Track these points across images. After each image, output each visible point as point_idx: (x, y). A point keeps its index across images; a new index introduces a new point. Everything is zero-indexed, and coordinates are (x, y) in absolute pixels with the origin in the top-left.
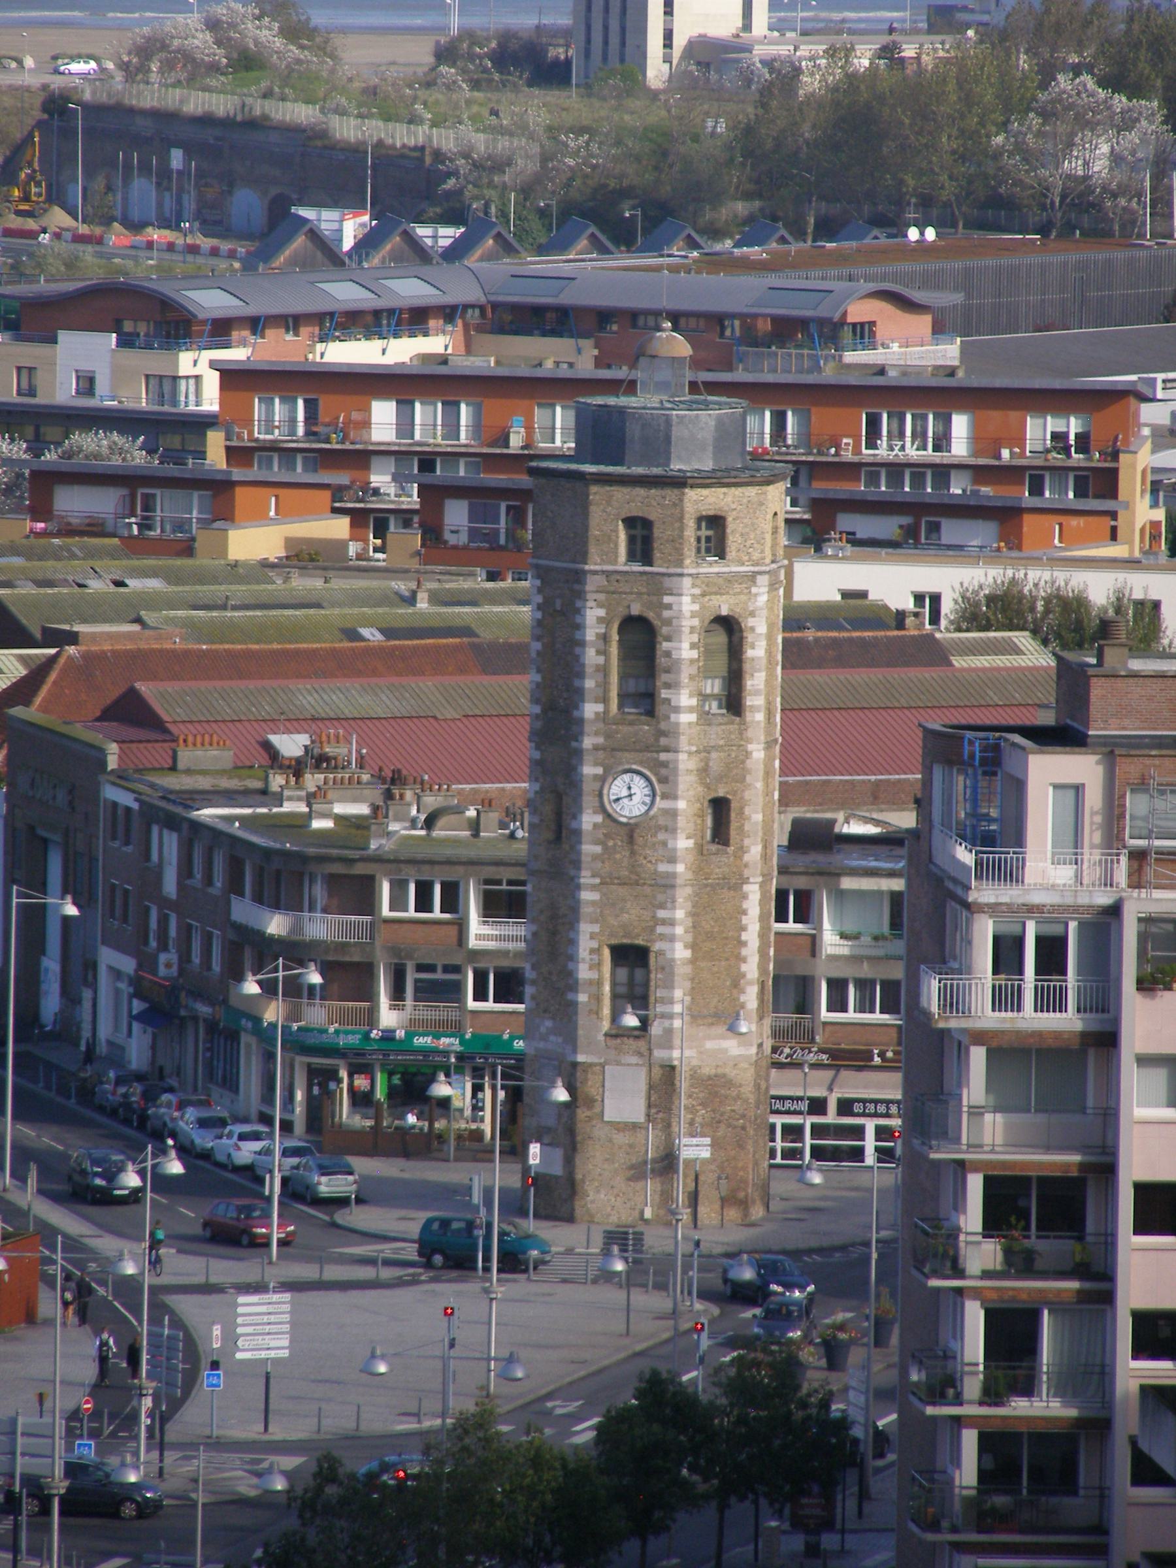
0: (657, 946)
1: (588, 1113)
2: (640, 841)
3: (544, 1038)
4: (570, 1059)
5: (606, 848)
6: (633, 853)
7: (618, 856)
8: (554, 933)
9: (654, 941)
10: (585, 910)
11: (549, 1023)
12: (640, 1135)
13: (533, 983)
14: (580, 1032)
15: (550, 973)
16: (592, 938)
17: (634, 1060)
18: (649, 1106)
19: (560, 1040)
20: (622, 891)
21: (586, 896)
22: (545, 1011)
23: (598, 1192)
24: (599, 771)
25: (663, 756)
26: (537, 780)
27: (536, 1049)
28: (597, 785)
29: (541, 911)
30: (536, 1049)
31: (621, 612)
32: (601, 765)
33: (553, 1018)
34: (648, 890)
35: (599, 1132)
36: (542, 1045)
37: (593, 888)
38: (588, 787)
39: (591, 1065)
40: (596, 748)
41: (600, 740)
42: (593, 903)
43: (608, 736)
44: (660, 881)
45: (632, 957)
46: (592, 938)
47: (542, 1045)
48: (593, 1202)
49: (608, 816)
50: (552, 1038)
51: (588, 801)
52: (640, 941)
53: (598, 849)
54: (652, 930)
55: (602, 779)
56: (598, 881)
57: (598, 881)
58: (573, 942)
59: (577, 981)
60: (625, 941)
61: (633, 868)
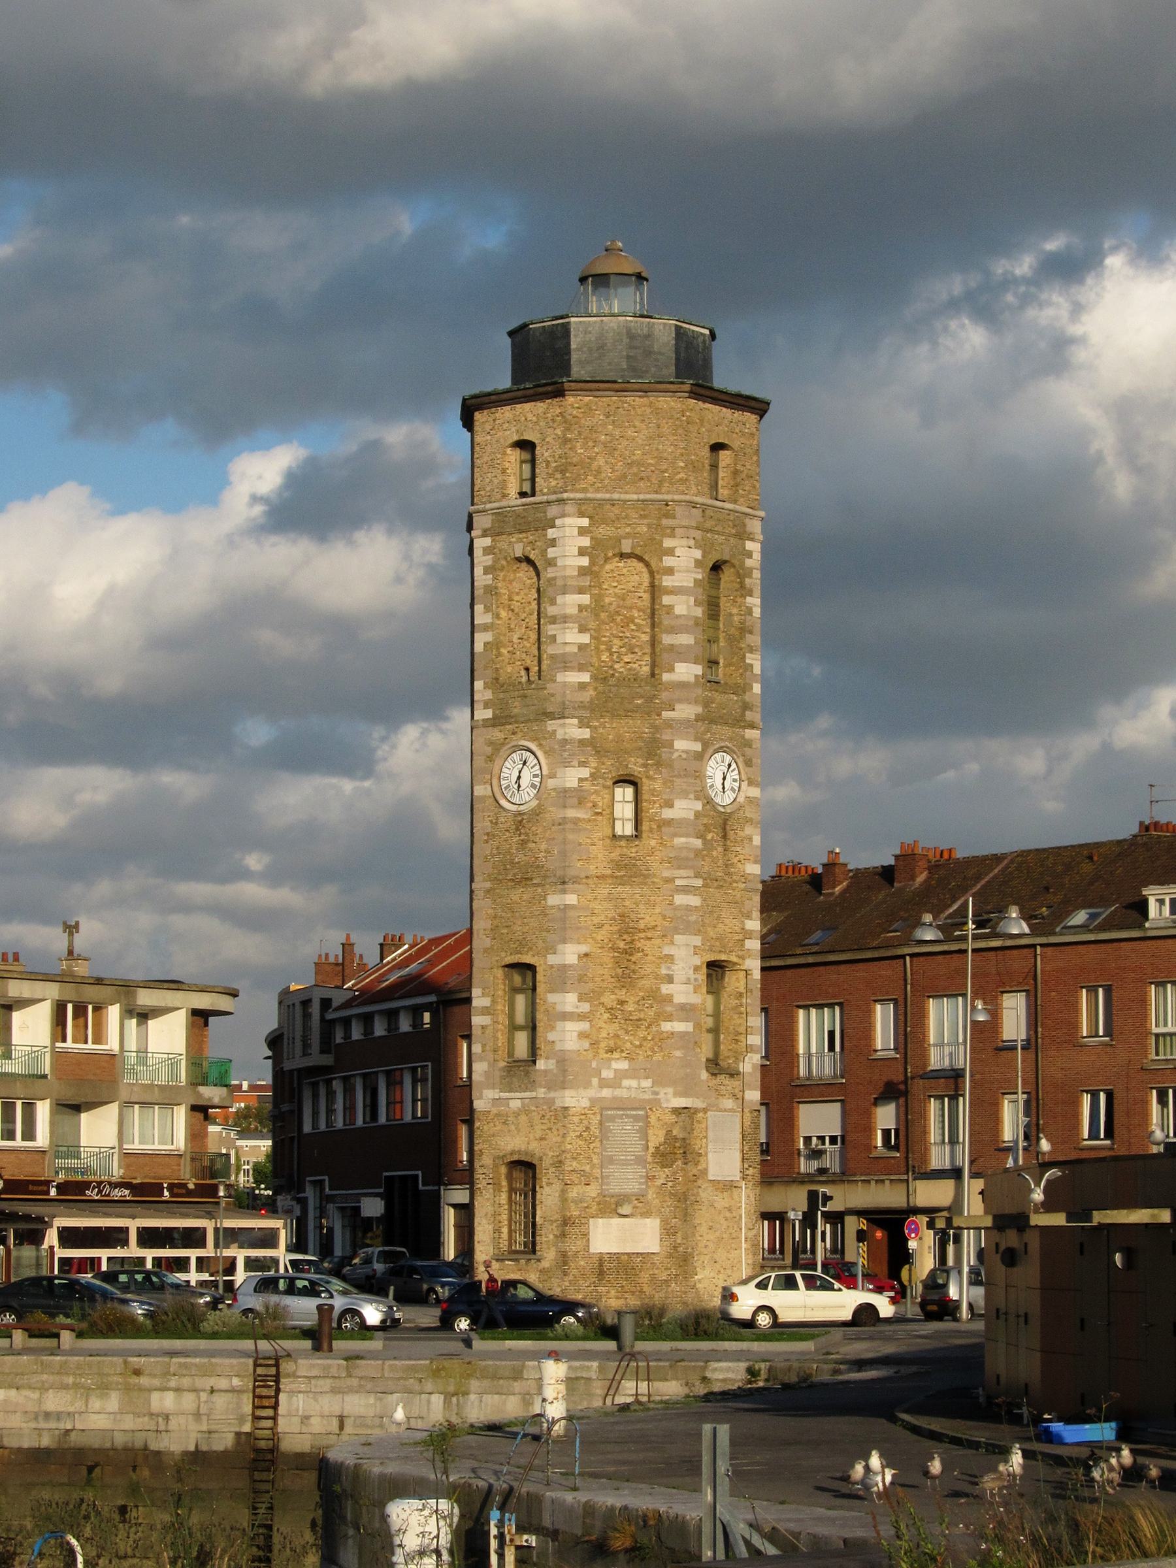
1: (695, 1171)
3: (604, 1084)
7: (714, 853)
8: (628, 952)
9: (743, 958)
11: (623, 1065)
12: (735, 1192)
13: (581, 1017)
19: (647, 1083)
22: (611, 1051)
24: (698, 747)
26: (582, 764)
33: (629, 1058)
36: (606, 1093)
47: (606, 1093)
48: (700, 1281)
50: (634, 1083)
52: (734, 959)
55: (700, 757)
56: (699, 882)
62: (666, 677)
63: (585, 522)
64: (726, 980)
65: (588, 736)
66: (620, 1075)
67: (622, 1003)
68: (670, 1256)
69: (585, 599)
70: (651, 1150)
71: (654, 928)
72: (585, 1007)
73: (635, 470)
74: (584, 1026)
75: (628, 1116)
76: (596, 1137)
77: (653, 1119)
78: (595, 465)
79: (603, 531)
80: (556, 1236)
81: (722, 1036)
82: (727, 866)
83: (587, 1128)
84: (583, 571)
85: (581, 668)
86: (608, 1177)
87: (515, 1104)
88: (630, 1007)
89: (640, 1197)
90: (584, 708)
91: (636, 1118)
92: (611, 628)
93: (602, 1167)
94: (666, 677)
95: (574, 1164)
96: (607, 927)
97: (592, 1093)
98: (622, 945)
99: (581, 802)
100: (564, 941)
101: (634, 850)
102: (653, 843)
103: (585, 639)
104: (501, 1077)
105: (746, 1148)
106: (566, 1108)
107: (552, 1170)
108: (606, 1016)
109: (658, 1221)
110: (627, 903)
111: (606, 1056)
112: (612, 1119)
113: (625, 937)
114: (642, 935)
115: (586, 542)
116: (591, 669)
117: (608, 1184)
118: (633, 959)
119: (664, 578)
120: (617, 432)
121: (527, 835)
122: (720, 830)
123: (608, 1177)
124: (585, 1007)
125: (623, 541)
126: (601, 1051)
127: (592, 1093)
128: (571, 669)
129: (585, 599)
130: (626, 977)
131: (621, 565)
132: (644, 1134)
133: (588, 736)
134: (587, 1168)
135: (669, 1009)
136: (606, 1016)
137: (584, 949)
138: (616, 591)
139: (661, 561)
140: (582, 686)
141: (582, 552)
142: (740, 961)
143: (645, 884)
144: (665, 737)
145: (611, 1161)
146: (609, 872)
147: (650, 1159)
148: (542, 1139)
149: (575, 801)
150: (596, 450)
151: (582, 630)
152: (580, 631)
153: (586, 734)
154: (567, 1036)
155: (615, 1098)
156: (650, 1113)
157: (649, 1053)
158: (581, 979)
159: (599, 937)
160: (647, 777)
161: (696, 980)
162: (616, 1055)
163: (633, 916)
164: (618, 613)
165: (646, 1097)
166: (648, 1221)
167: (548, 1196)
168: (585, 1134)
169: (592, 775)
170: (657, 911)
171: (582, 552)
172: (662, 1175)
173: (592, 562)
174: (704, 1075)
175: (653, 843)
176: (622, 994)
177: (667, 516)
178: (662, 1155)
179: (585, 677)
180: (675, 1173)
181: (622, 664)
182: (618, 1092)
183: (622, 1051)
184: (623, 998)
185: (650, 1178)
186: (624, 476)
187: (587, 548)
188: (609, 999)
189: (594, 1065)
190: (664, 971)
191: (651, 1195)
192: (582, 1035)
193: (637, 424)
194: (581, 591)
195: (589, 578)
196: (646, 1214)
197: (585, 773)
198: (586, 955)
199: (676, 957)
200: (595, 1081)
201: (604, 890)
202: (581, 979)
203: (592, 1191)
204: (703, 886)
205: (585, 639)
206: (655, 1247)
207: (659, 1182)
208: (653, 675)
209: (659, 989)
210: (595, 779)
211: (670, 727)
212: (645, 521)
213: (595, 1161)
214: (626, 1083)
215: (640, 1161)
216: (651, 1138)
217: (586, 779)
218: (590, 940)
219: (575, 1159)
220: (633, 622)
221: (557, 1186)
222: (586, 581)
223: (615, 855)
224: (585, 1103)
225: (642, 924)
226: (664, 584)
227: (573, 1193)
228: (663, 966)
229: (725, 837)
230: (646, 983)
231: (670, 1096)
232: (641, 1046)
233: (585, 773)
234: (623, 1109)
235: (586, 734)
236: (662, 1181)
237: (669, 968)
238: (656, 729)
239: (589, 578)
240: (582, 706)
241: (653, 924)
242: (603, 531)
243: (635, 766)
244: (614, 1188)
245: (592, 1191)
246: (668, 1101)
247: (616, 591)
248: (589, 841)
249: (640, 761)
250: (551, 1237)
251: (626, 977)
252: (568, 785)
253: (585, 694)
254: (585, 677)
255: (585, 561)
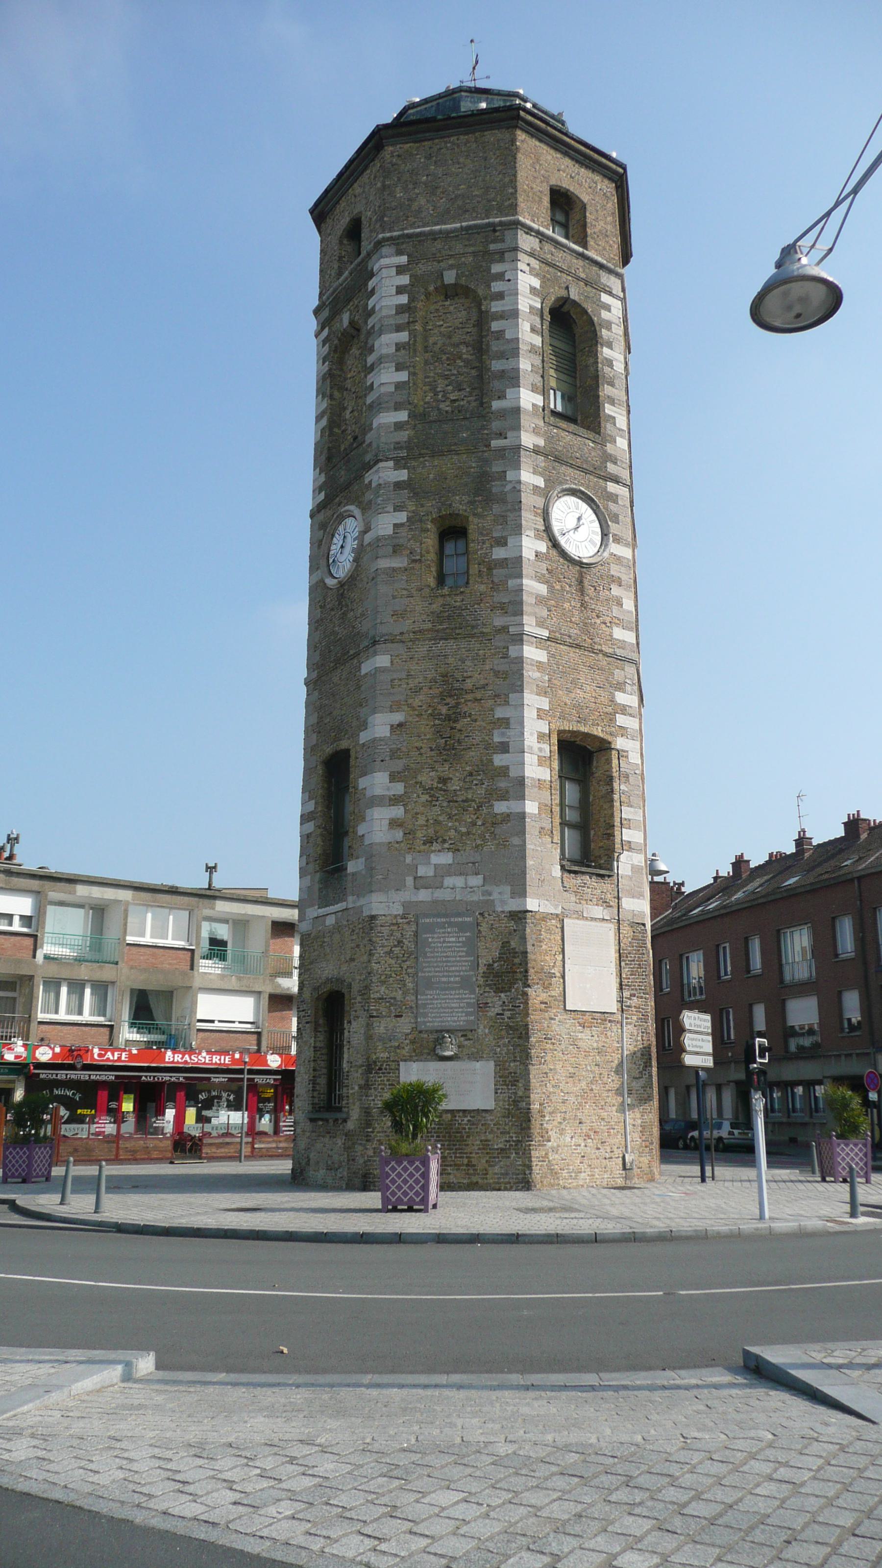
0: (620, 743)
1: (543, 996)
2: (591, 591)
3: (420, 883)
4: (513, 905)
5: (551, 588)
6: (584, 605)
8: (453, 718)
10: (531, 674)
11: (445, 858)
13: (394, 801)
14: (530, 862)
15: (444, 780)
16: (539, 717)
17: (598, 911)
18: (621, 987)
19: (476, 881)
20: (573, 655)
21: (532, 653)
22: (429, 841)
23: (562, 1132)
25: (612, 487)
26: (398, 509)
27: (405, 905)
28: (540, 502)
29: (417, 690)
30: (405, 905)
31: (557, 292)
32: (541, 474)
34: (604, 661)
35: (560, 1026)
36: (424, 895)
37: (540, 642)
38: (528, 500)
39: (545, 917)
40: (537, 451)
41: (541, 442)
42: (539, 665)
43: (549, 439)
44: (619, 652)
45: (583, 758)
46: (539, 717)
47: (424, 895)
48: (555, 1150)
49: (555, 544)
50: (459, 881)
51: (529, 520)
52: (598, 732)
53: (543, 589)
54: (612, 720)
57: (546, 633)
58: (512, 723)
59: (521, 782)
60: (583, 729)
61: (586, 627)
62: (496, 405)
63: (404, 259)
64: (595, 763)
65: (405, 478)
66: (442, 872)
67: (444, 780)
68: (508, 1114)
69: (404, 336)
70: (482, 969)
71: (483, 687)
72: (399, 788)
73: (460, 203)
74: (398, 812)
75: (451, 924)
76: (411, 953)
77: (484, 928)
78: (415, 206)
79: (422, 268)
80: (361, 1087)
81: (592, 832)
82: (585, 624)
83: (399, 942)
84: (401, 309)
85: (397, 407)
86: (425, 1006)
87: (330, 921)
88: (454, 785)
89: (466, 1033)
90: (401, 448)
91: (462, 927)
92: (435, 368)
93: (416, 994)
94: (496, 405)
95: (383, 989)
96: (425, 690)
97: (408, 895)
98: (444, 710)
99: (396, 550)
100: (374, 711)
101: (459, 598)
102: (482, 588)
103: (403, 376)
104: (320, 889)
105: (626, 971)
106: (373, 918)
107: (359, 999)
108: (425, 798)
109: (492, 1064)
110: (451, 660)
111: (423, 847)
112: (430, 929)
113: (448, 700)
114: (469, 697)
115: (405, 280)
116: (409, 407)
117: (425, 1015)
118: (458, 726)
119: (493, 303)
120: (440, 171)
121: (347, 606)
122: (574, 582)
123: (425, 1006)
124: (399, 788)
125: (444, 273)
126: (419, 842)
127: (408, 895)
128: (388, 410)
129: (404, 336)
130: (449, 747)
131: (447, 303)
132: (471, 947)
133: (405, 478)
134: (399, 995)
135: (503, 784)
136: (425, 798)
137: (398, 717)
138: (442, 329)
139: (489, 287)
140: (399, 426)
141: (400, 290)
142: (609, 738)
143: (473, 636)
144: (495, 469)
145: (429, 984)
146: (430, 625)
147: (481, 981)
148: (352, 960)
149: (390, 549)
150: (417, 191)
151: (399, 368)
152: (397, 370)
153: (403, 475)
154: (377, 826)
155: (435, 902)
156: (480, 918)
157: (479, 842)
158: (394, 754)
159: (416, 702)
160: (475, 515)
161: (540, 750)
162: (436, 847)
163: (458, 675)
164: (443, 351)
165: (475, 898)
166: (478, 1065)
167: (354, 1032)
168: (397, 950)
169: (409, 519)
170: (487, 667)
171: (400, 290)
172: (496, 1003)
173: (412, 299)
174: (557, 871)
175: (482, 588)
176: (444, 770)
177: (494, 241)
178: (497, 975)
179: (403, 416)
180: (514, 999)
181: (448, 403)
182: (440, 895)
183: (444, 841)
184: (446, 774)
185: (482, 1006)
186: (448, 211)
187: (406, 286)
188: (427, 778)
189: (409, 859)
190: (497, 739)
191: (482, 1030)
192: (394, 823)
193: (461, 160)
194: (399, 329)
195: (407, 315)
196: (476, 1057)
197: (402, 517)
198: (400, 725)
199: (512, 721)
200: (409, 881)
201: (422, 649)
202: (394, 754)
203: (404, 1026)
204: (549, 639)
205: (403, 376)
206: (488, 1103)
207: (492, 1012)
208: (482, 404)
209: (491, 761)
210: (413, 523)
211: (503, 457)
212: (471, 249)
213: (410, 985)
214: (449, 881)
215: (465, 984)
216: (482, 952)
217: (402, 525)
218: (406, 708)
219: (383, 983)
220: (460, 358)
221: (362, 1021)
222: (404, 318)
223: (436, 607)
224: (397, 910)
225: (469, 684)
226: (493, 310)
227: (381, 1028)
228: (496, 732)
229: (582, 591)
230: (473, 755)
231: (507, 896)
232: (468, 833)
233: (402, 517)
234: (446, 916)
235: (403, 475)
236: (498, 1010)
237: (503, 734)
238: (486, 462)
239: (407, 315)
240: (398, 446)
241: (482, 682)
242: (422, 268)
243: (459, 504)
244: (432, 1021)
245: (404, 1026)
246: (503, 902)
247: (442, 329)
248: (405, 592)
249: (466, 499)
250: (357, 1088)
251: (449, 747)
252: (381, 533)
253: (402, 433)
254: (403, 416)
255: (404, 299)
